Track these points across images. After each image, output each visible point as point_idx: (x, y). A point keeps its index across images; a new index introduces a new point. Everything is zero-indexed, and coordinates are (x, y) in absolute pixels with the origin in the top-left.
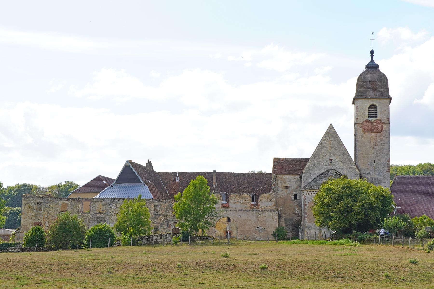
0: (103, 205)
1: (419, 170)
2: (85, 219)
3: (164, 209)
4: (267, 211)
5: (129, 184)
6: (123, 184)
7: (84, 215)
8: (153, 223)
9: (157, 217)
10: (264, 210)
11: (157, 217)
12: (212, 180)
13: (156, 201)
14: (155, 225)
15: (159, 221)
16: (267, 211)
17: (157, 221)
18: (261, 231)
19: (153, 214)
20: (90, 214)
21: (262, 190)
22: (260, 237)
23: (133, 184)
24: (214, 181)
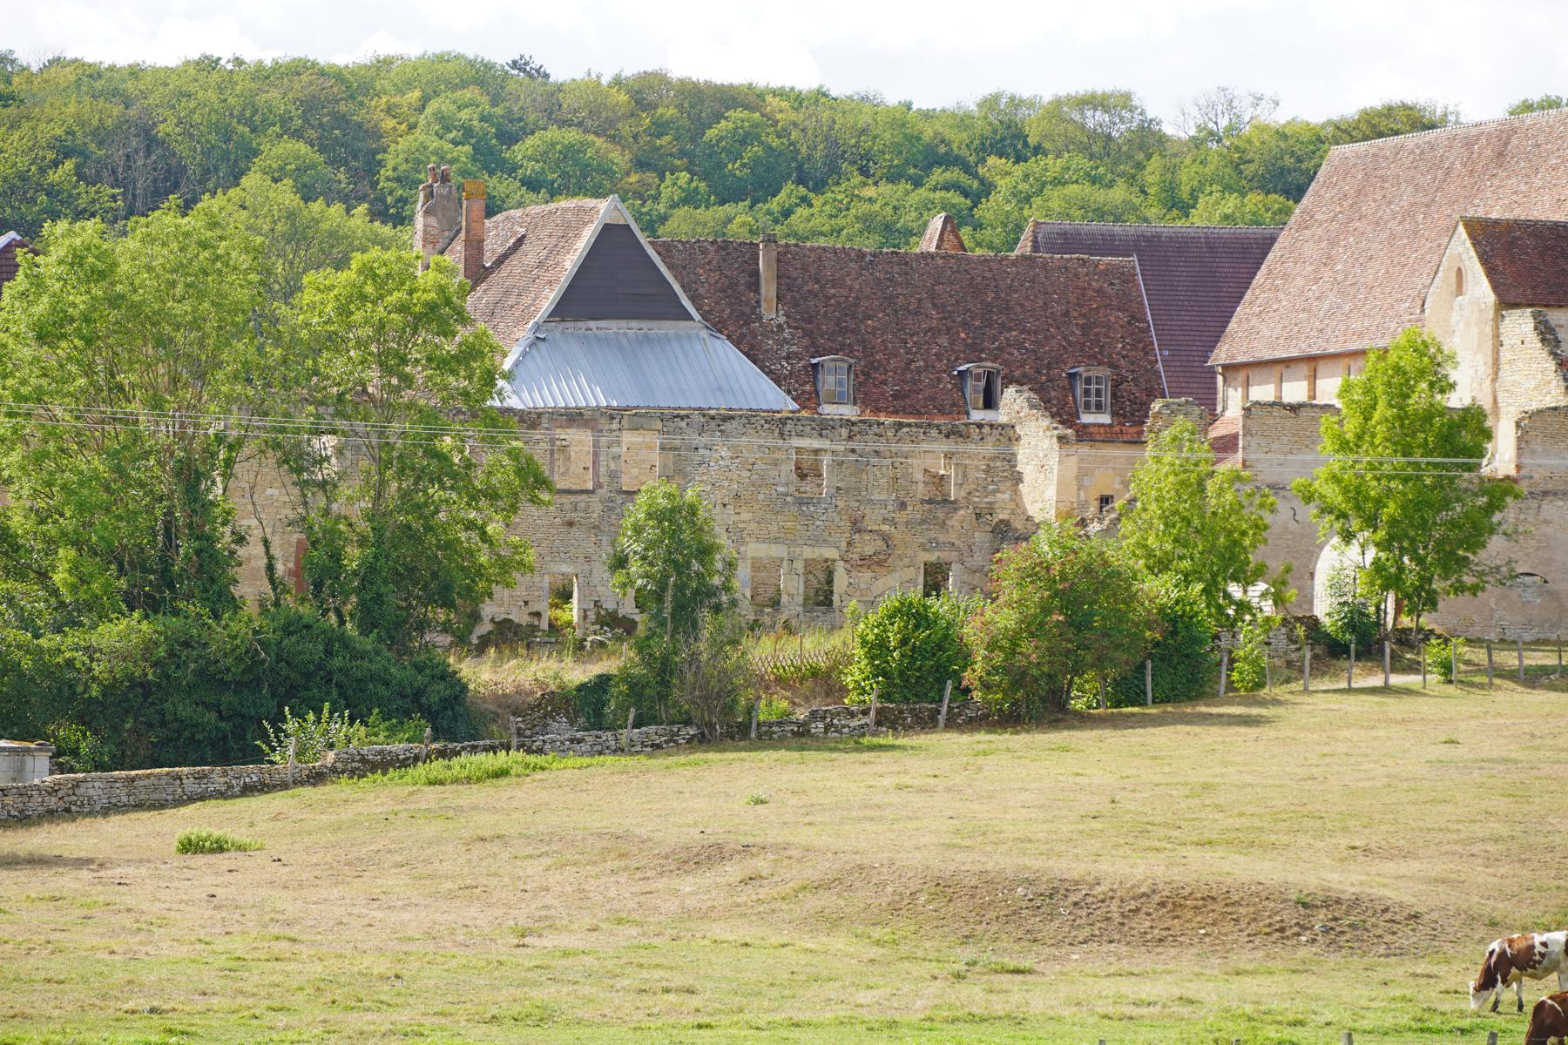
0: (663, 448)
1: (272, 96)
2: (571, 524)
3: (972, 474)
4: (1555, 494)
5: (623, 323)
6: (592, 324)
7: (566, 499)
8: (923, 547)
9: (940, 515)
10: (1545, 493)
11: (940, 515)
12: (755, 286)
13: (934, 433)
14: (932, 557)
15: (953, 537)
16: (1555, 494)
17: (942, 538)
18: (1528, 596)
19: (923, 502)
20: (595, 498)
21: (1020, 345)
22: (1528, 625)
23: (645, 324)
24: (768, 289)
